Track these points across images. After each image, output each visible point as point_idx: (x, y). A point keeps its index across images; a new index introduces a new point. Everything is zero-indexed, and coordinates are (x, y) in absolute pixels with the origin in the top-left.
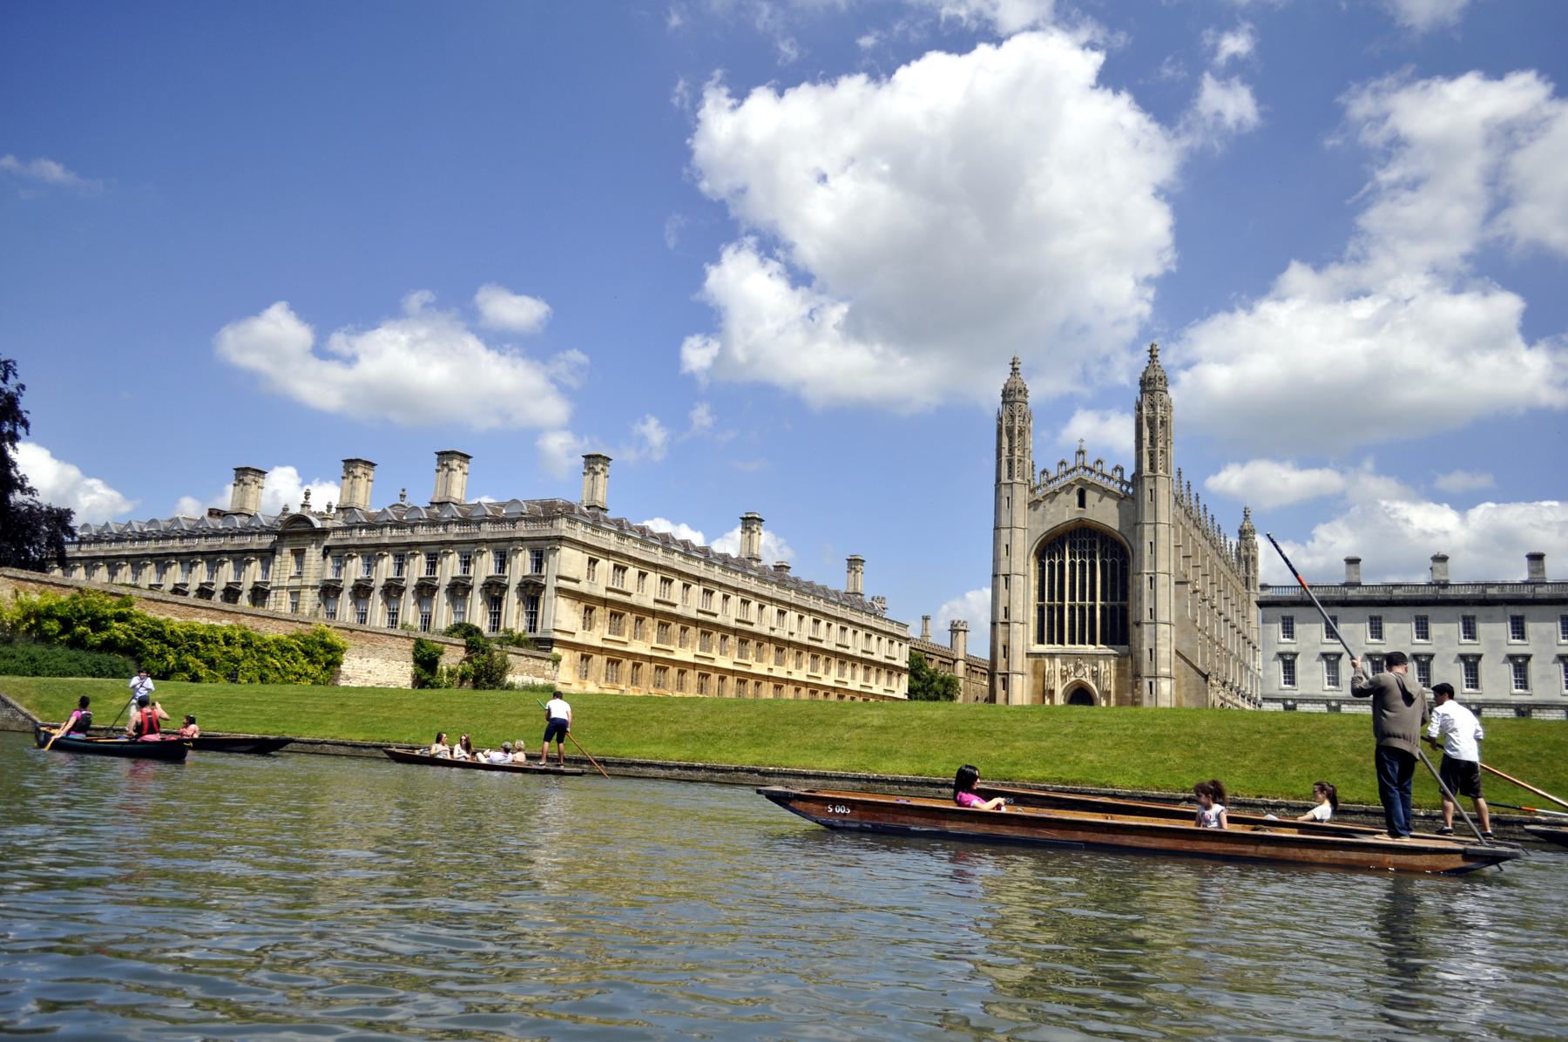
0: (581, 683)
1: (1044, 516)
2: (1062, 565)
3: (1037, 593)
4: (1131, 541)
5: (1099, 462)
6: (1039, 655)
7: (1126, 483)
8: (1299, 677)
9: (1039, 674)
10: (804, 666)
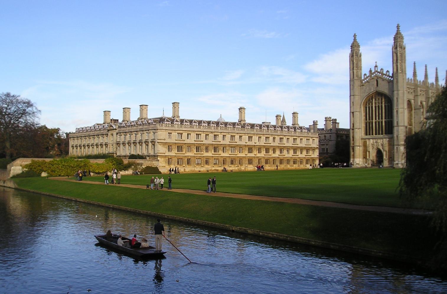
0: (168, 166)
3: (365, 117)
5: (382, 69)
6: (365, 139)
9: (365, 145)
10: (263, 152)
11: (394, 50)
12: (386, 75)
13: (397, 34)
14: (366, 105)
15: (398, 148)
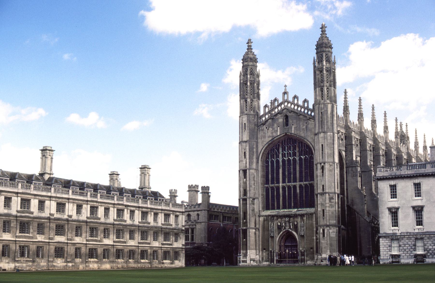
2: (278, 162)
5: (295, 97)
8: (400, 222)
11: (317, 64)
12: (302, 107)
14: (266, 159)
15: (326, 231)
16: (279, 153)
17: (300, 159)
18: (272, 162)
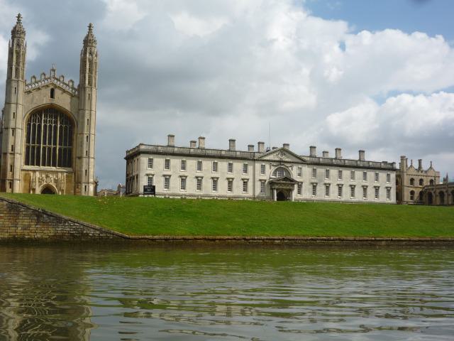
1: (32, 99)
2: (40, 126)
4: (76, 116)
6: (28, 170)
7: (75, 89)
12: (67, 85)
13: (87, 37)
16: (41, 119)
17: (61, 127)
18: (34, 125)
